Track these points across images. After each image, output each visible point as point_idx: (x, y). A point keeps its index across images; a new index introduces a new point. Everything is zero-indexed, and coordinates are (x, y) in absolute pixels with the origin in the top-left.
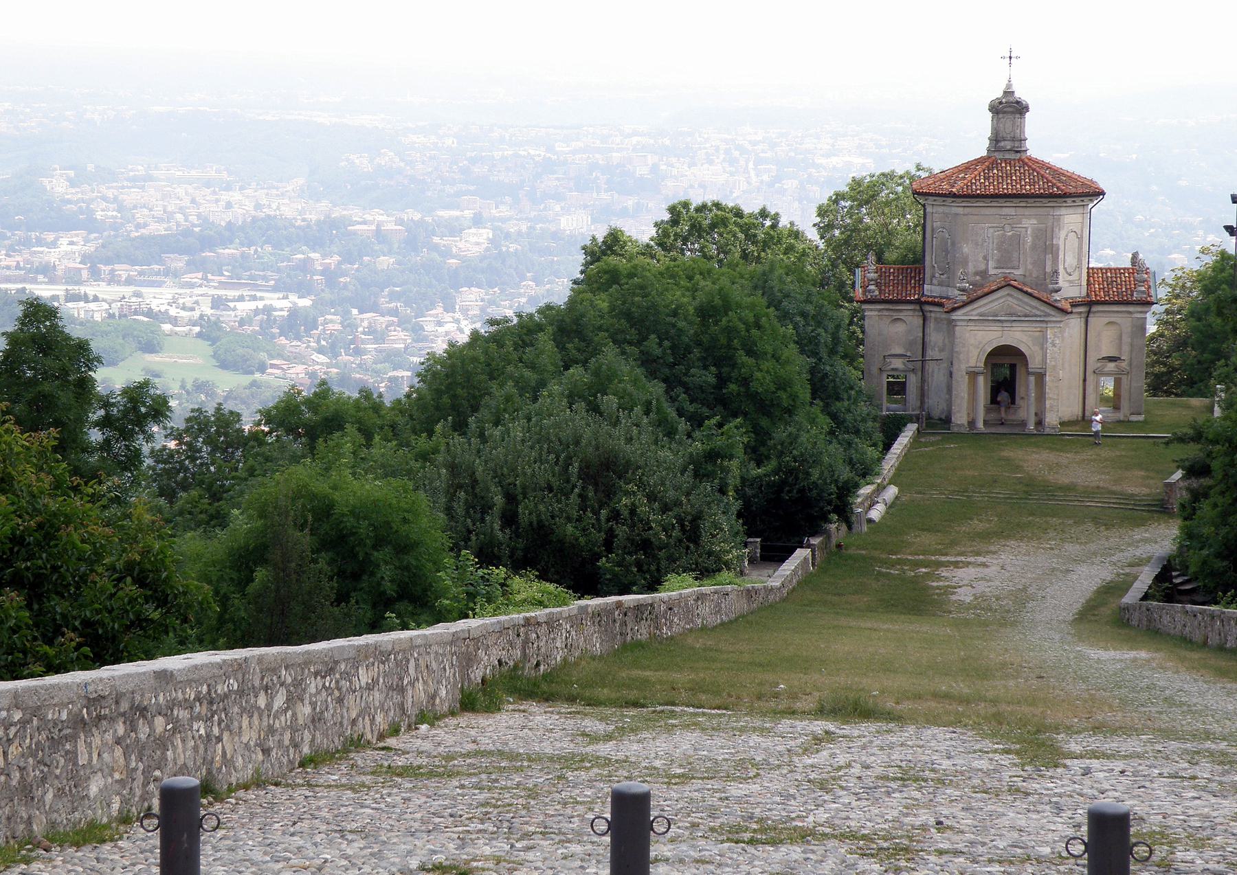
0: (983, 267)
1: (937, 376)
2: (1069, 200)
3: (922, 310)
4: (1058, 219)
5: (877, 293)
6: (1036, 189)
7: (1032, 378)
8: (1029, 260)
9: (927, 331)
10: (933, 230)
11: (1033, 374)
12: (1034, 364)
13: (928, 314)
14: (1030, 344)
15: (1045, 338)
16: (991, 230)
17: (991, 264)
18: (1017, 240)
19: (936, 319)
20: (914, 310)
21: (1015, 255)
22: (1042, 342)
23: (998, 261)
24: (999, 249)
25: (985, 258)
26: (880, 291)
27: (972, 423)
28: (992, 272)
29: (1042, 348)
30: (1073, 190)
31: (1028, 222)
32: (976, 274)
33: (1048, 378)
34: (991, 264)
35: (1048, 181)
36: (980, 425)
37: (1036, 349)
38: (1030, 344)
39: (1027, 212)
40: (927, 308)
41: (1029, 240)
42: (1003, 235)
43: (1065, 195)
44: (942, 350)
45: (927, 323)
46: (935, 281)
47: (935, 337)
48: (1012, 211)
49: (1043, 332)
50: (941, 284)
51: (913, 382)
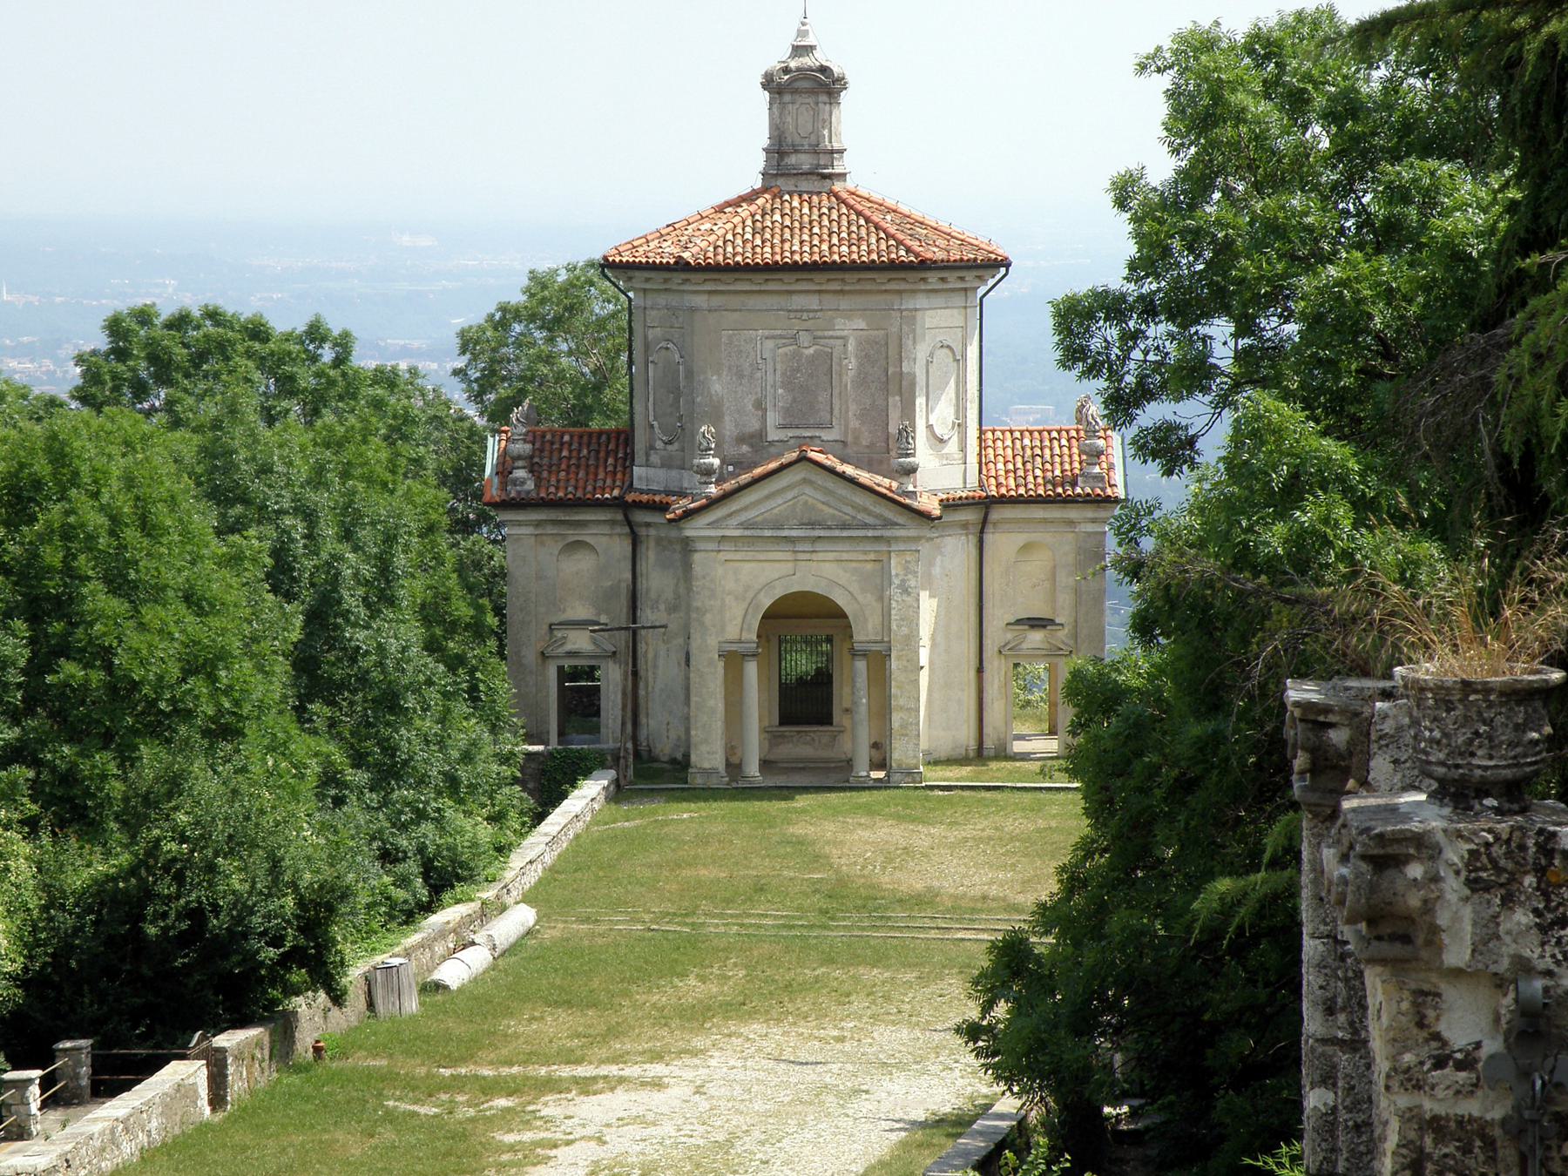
0: (754, 425)
1: (661, 668)
2: (933, 277)
3: (630, 524)
4: (910, 318)
5: (530, 485)
6: (861, 254)
7: (861, 665)
8: (853, 407)
9: (642, 567)
10: (647, 346)
11: (865, 655)
12: (865, 631)
13: (642, 531)
14: (855, 588)
15: (885, 574)
16: (770, 344)
17: (773, 418)
18: (826, 364)
19: (659, 541)
20: (613, 523)
21: (823, 397)
22: (880, 584)
23: (787, 412)
24: (788, 384)
25: (759, 405)
26: (539, 482)
27: (734, 768)
28: (773, 435)
29: (881, 598)
30: (940, 255)
31: (848, 328)
32: (741, 439)
33: (894, 664)
34: (773, 418)
35: (889, 236)
36: (753, 769)
37: (868, 599)
38: (855, 588)
39: (844, 302)
40: (640, 517)
41: (852, 364)
42: (796, 355)
43: (924, 265)
44: (673, 609)
45: (642, 549)
46: (654, 458)
47: (657, 581)
48: (812, 302)
49: (882, 564)
50: (667, 464)
51: (612, 679)
